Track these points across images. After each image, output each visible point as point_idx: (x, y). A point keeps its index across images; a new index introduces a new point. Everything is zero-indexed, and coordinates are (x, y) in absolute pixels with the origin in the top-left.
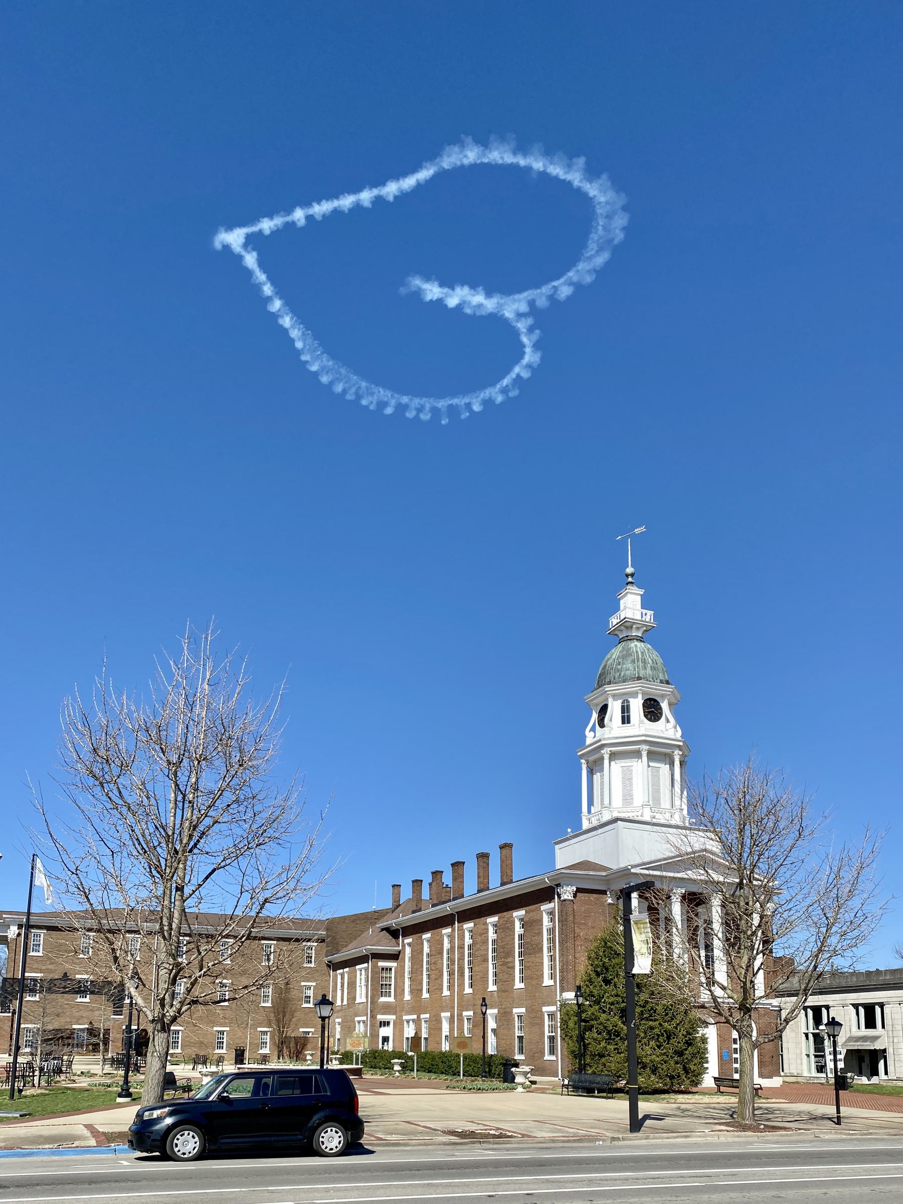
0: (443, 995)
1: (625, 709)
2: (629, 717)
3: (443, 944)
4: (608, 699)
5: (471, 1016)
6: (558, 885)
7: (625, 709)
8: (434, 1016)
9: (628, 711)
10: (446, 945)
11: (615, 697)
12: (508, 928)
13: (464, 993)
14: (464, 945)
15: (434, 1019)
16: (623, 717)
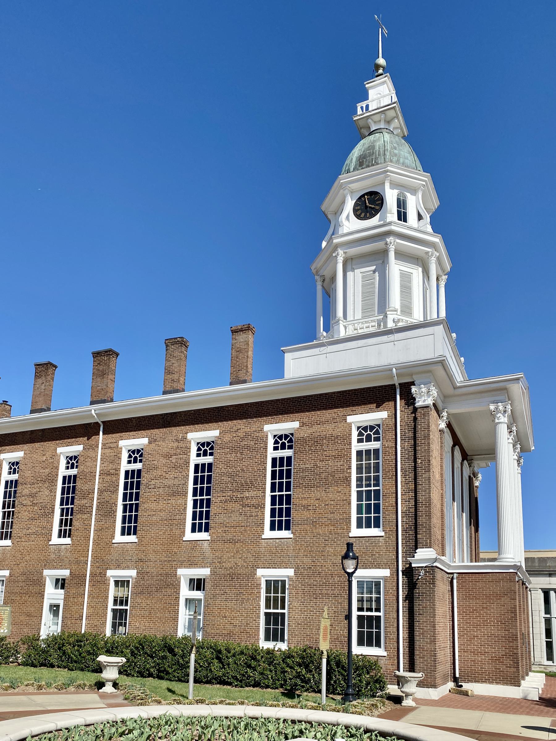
0: (50, 543)
1: (401, 204)
2: (405, 214)
3: (57, 468)
4: (384, 183)
5: (131, 577)
6: (413, 383)
7: (401, 204)
8: (23, 574)
9: (405, 207)
10: (63, 471)
11: (394, 185)
12: (248, 447)
13: (114, 541)
14: (118, 470)
15: (24, 578)
16: (399, 213)
